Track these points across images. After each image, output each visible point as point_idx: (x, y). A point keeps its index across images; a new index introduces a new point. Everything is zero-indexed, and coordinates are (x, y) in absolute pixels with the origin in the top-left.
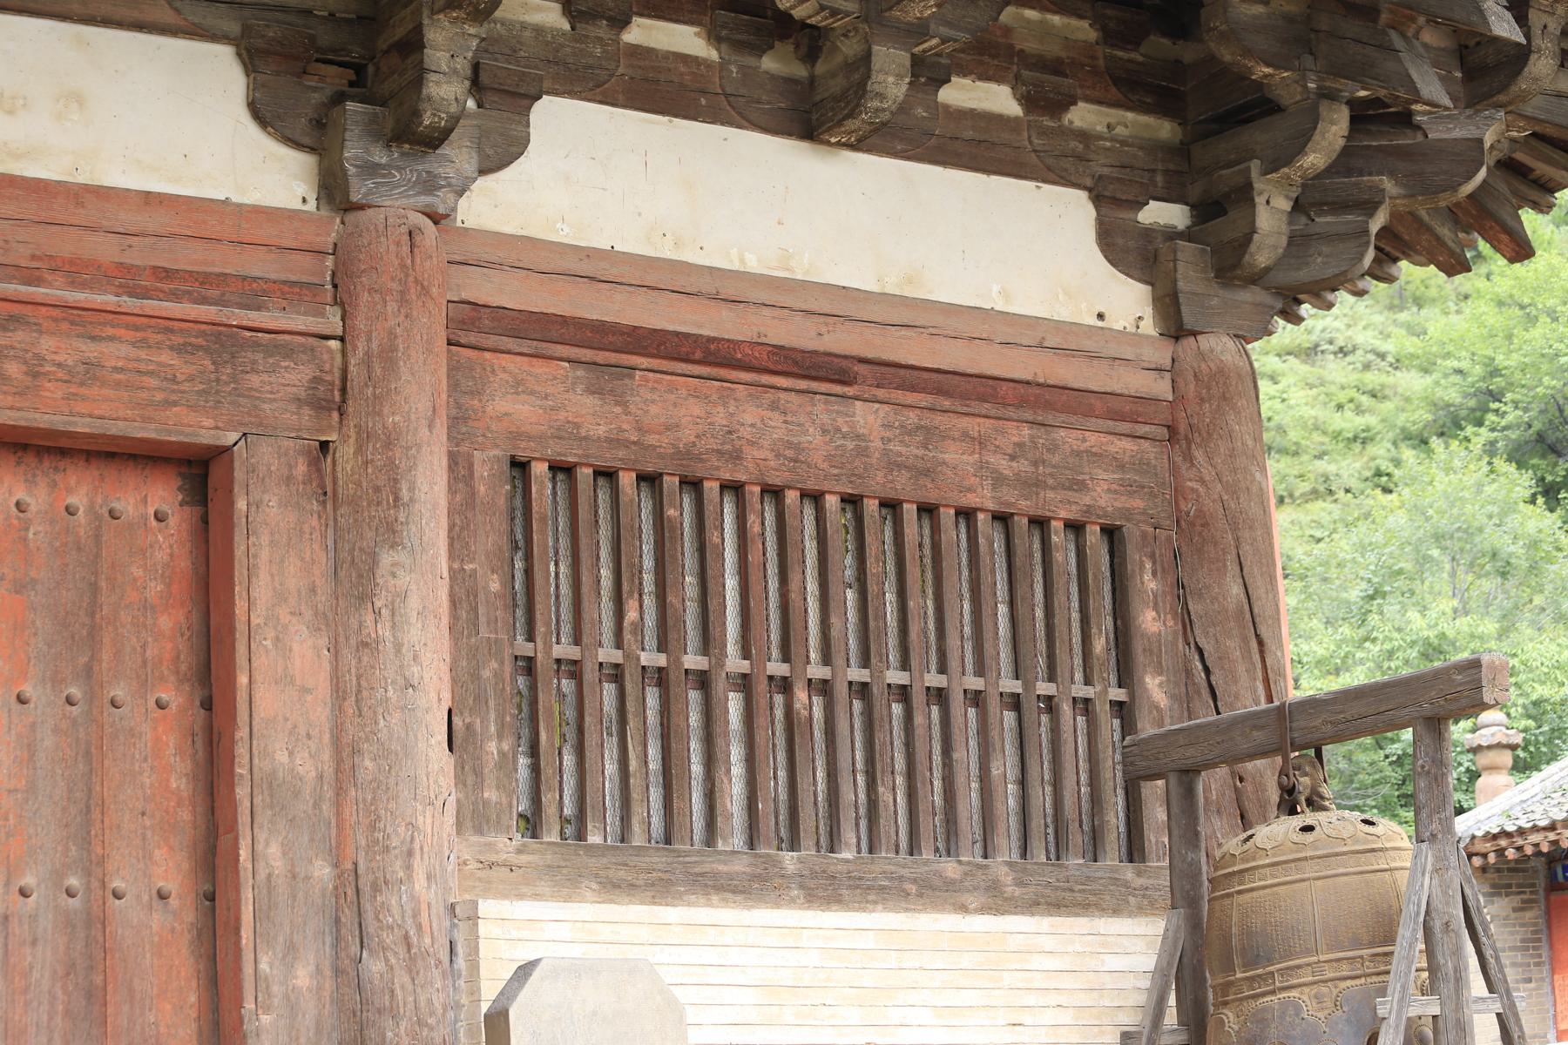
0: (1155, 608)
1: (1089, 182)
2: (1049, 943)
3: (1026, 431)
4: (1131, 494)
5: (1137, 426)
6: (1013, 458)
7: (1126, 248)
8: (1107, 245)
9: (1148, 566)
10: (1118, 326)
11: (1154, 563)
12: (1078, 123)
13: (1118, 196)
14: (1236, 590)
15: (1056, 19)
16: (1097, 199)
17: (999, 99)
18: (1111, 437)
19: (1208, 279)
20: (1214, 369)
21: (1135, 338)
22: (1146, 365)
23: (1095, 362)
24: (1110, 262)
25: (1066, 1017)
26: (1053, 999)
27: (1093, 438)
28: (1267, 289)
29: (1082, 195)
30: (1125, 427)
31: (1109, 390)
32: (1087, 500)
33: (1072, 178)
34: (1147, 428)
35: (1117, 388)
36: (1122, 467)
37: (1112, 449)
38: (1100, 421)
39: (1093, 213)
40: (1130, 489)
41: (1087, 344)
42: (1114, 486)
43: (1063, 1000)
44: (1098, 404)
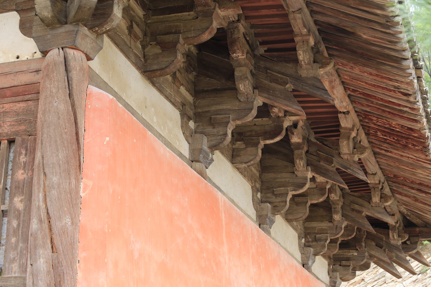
0: (24, 168)
1: (14, 7)
4: (20, 125)
5: (25, 97)
8: (23, 28)
9: (24, 152)
10: (25, 59)
11: (27, 150)
13: (24, 8)
18: (14, 104)
19: (46, 29)
20: (46, 64)
22: (31, 71)
23: (8, 76)
24: (23, 34)
27: (6, 106)
28: (71, 23)
29: (15, 13)
30: (20, 98)
31: (12, 85)
33: (8, 8)
34: (30, 96)
35: (16, 83)
36: (18, 114)
37: (15, 108)
38: (9, 99)
40: (19, 122)
41: (7, 70)
42: (13, 123)
44: (8, 93)
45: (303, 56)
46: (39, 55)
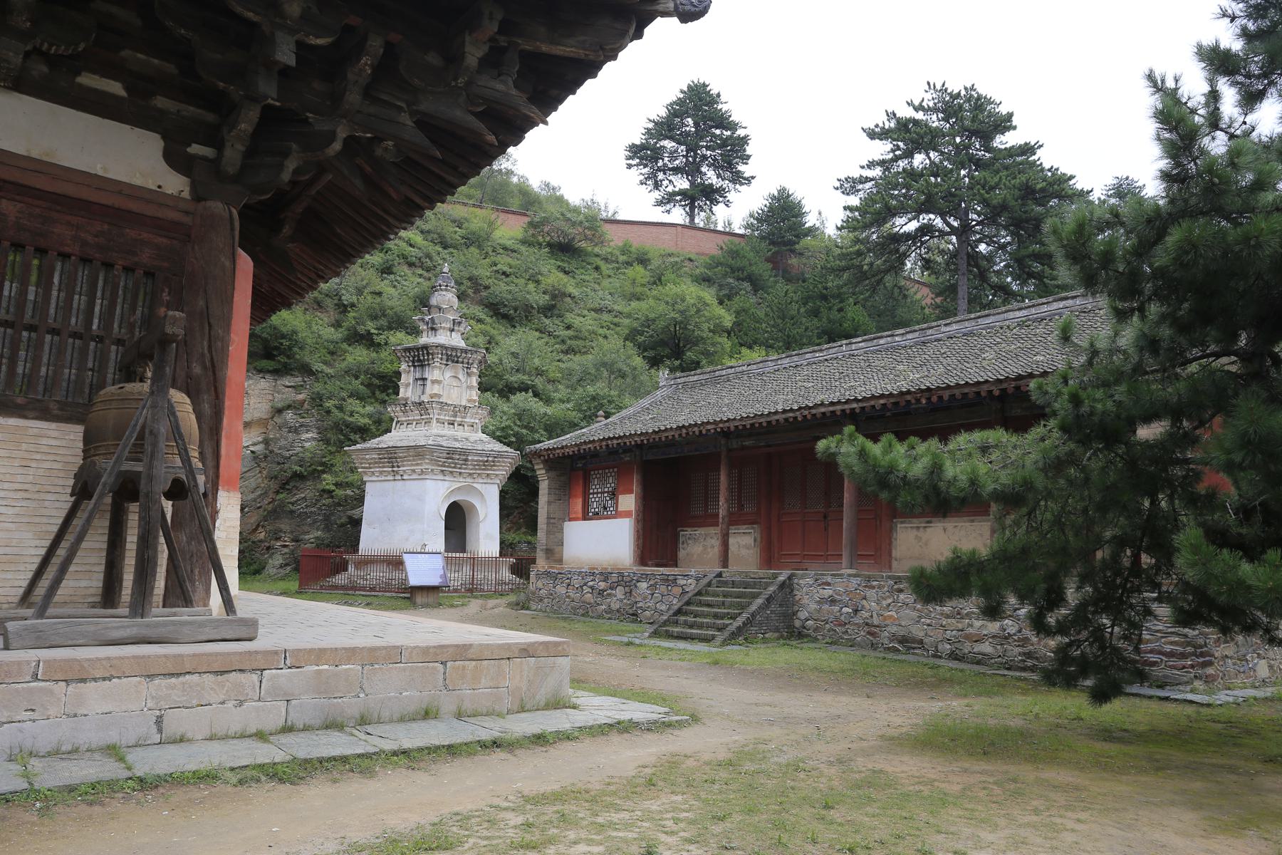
2: (55, 434)
3: (106, 227)
6: (96, 236)
7: (175, 159)
10: (170, 192)
12: (159, 105)
14: (201, 303)
15: (156, 61)
16: (164, 138)
17: (116, 88)
21: (176, 198)
25: (58, 466)
26: (51, 457)
29: (158, 136)
32: (136, 259)
39: (162, 144)
43: (58, 458)
45: (287, 230)
46: (186, 194)
